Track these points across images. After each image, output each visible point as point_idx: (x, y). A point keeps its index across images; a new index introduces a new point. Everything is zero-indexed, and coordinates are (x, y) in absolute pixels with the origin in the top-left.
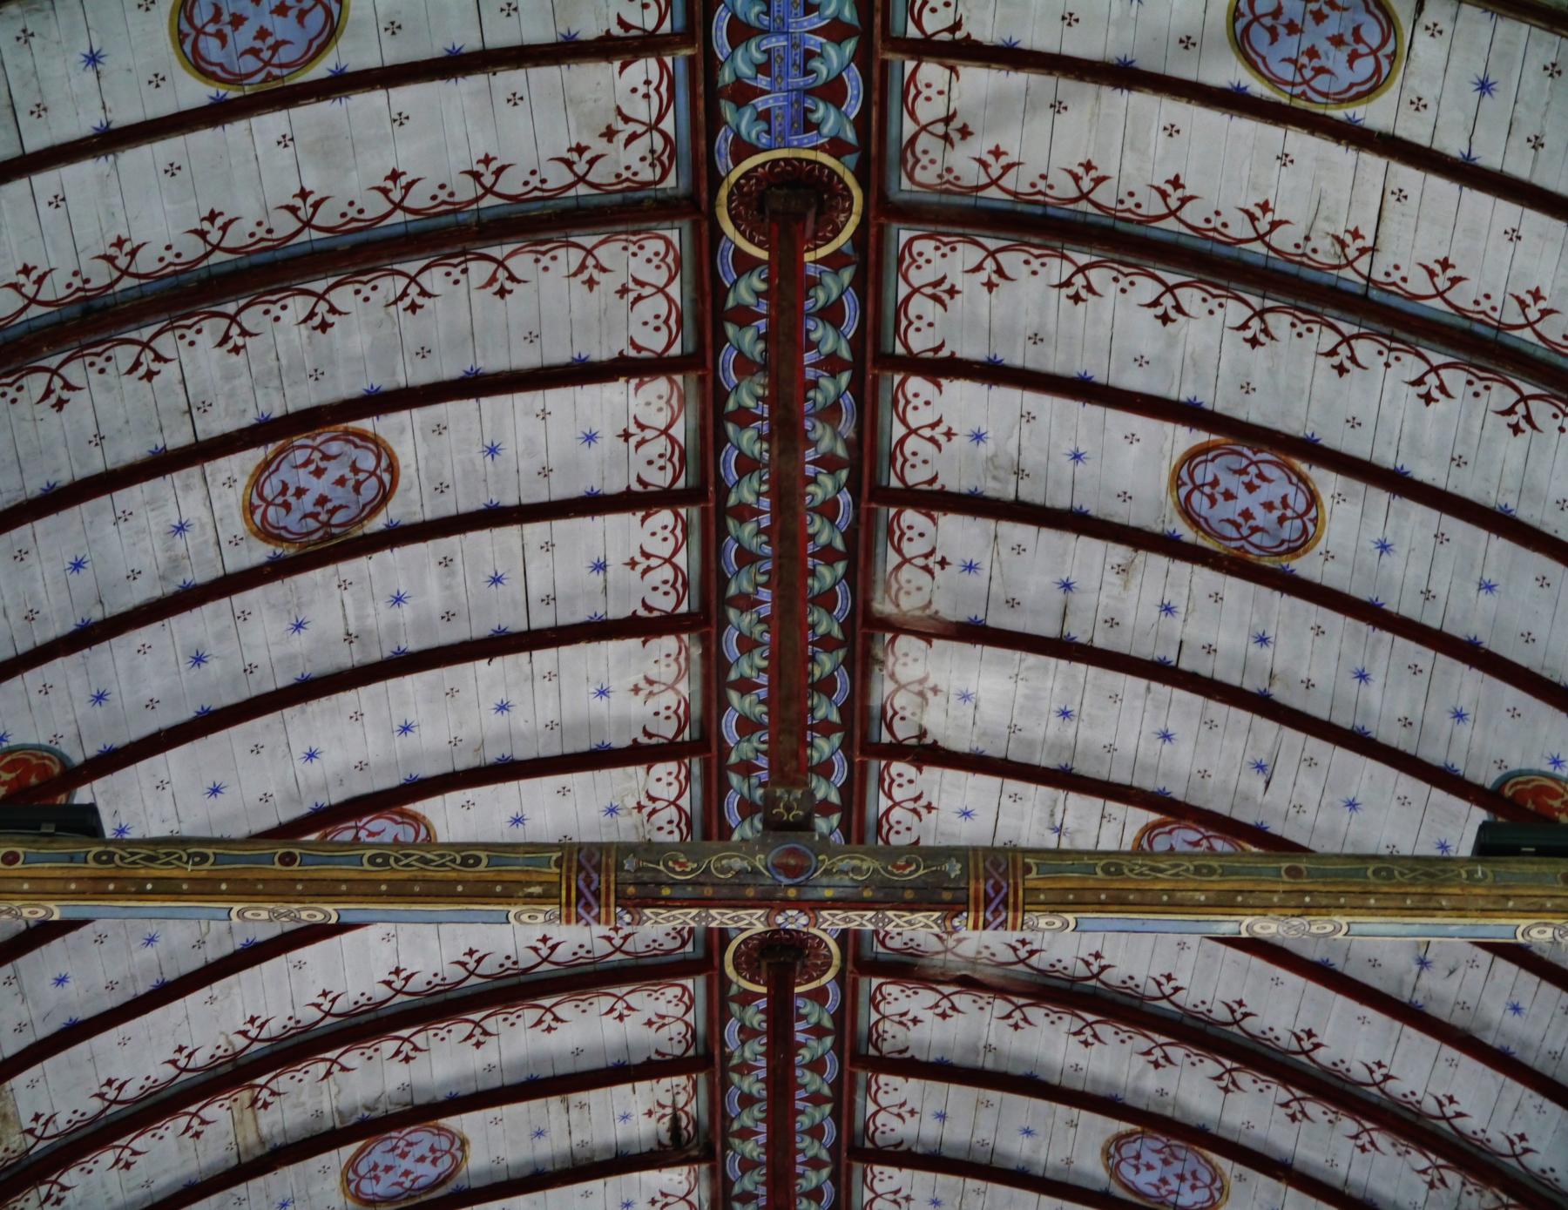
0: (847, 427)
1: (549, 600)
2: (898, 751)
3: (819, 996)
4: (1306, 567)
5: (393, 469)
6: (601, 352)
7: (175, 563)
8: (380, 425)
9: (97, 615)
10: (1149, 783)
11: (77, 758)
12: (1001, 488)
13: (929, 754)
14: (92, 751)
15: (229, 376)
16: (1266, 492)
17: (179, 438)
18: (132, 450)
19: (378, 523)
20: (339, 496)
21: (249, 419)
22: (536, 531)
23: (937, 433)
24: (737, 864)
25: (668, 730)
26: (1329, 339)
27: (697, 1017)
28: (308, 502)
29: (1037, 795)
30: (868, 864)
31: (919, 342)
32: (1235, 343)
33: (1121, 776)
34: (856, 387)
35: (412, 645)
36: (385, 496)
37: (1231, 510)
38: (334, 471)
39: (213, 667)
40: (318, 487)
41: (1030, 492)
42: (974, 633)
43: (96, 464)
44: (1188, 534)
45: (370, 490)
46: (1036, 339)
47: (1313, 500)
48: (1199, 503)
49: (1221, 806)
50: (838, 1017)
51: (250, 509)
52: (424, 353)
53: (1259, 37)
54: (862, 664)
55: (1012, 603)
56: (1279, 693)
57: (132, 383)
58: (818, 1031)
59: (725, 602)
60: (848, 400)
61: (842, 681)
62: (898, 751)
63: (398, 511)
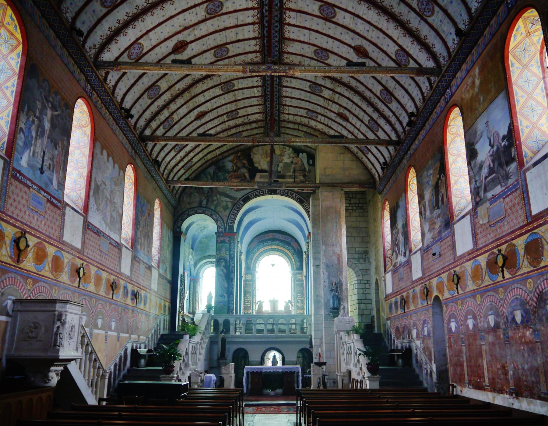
53: (220, 4)
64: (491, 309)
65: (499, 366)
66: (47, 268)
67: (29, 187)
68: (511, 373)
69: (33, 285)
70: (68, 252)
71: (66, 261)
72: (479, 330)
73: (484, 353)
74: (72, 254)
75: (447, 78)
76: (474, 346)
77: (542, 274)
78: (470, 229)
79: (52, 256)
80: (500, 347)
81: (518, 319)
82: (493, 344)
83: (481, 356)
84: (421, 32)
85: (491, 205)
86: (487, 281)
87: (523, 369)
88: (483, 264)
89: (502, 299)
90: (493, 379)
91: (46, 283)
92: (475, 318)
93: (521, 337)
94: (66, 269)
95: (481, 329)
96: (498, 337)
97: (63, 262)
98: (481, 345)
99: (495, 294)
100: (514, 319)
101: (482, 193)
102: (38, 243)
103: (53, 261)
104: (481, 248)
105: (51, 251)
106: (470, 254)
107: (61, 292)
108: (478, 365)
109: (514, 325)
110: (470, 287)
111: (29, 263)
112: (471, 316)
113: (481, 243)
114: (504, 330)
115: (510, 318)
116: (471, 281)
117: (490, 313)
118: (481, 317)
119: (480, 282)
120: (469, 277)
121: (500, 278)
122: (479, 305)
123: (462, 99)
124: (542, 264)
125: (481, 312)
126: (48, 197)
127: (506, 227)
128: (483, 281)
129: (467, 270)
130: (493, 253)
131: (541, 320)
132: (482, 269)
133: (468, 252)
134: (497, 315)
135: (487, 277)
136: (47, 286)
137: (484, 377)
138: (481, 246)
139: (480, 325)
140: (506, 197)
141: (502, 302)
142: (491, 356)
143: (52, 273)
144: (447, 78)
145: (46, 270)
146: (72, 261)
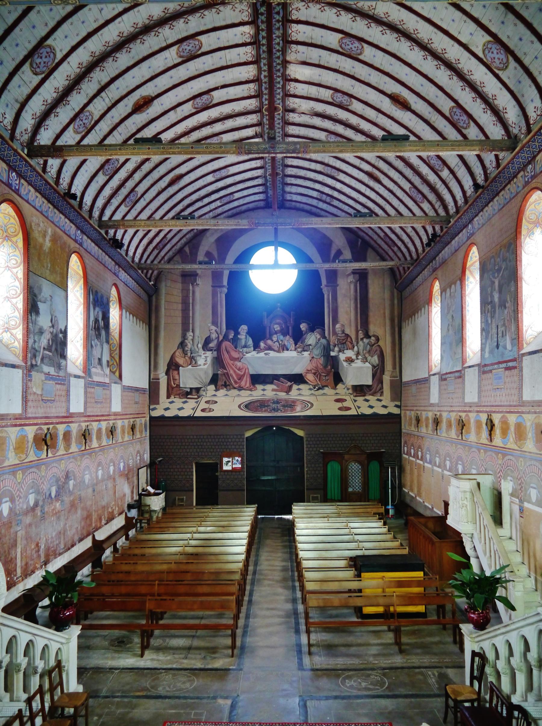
0: (281, 31)
1: (230, 60)
2: (292, 80)
3: (279, 114)
4: (361, 57)
5: (201, 44)
6: (237, 21)
7: (166, 64)
8: (199, 38)
9: (154, 74)
10: (334, 86)
11: (153, 95)
12: (309, 41)
13: (297, 81)
14: (156, 94)
15: (171, 33)
16: (354, 45)
17: (164, 44)
18: (156, 48)
19: (200, 52)
20: (192, 49)
21: (176, 40)
22: (227, 51)
23: (298, 32)
24: (264, 146)
25: (252, 78)
26: (367, 22)
27: (259, 118)
28: (187, 51)
29: (315, 88)
30: (285, 146)
31: (294, 17)
32: (350, 21)
33: (329, 85)
34: (283, 25)
35: (207, 69)
36: (200, 48)
37: (349, 47)
38: (191, 45)
39: (174, 79)
40: (188, 48)
41: (314, 42)
42: (304, 63)
43: (150, 51)
44: (341, 50)
45: (198, 47)
46: (315, 17)
47: (363, 47)
48: (343, 46)
49: (346, 91)
50: (282, 117)
51: (177, 54)
52: (205, 25)
54: (285, 68)
55: (311, 59)
56: (356, 76)
57: (155, 38)
58: (279, 119)
59: (260, 58)
60: (281, 27)
61: (282, 70)
62: (292, 80)
63: (203, 50)
64: (32, 488)
65: (33, 547)
66: (511, 440)
67: (491, 371)
68: (43, 547)
69: (503, 459)
70: (529, 413)
71: (528, 424)
72: (16, 514)
73: (19, 540)
74: (535, 413)
75: (29, 173)
76: (7, 538)
77: (69, 458)
78: (21, 388)
79: (514, 425)
80: (36, 527)
81: (53, 495)
82: (30, 525)
83: (15, 545)
84: (63, 109)
85: (46, 380)
86: (32, 457)
87: (52, 538)
88: (31, 437)
89: (43, 476)
90: (27, 564)
91: (512, 455)
92: (12, 500)
93: (53, 510)
94: (530, 435)
95: (18, 512)
96: (35, 516)
97: (525, 427)
98: (16, 532)
99: (37, 471)
100: (50, 494)
101: (39, 359)
102: (502, 417)
103: (515, 429)
104: (29, 418)
105: (512, 419)
106: (17, 419)
107: (528, 464)
108: (9, 559)
109: (49, 501)
110: (11, 460)
111: (498, 440)
112: (8, 499)
113: (31, 412)
114: (42, 507)
115: (47, 495)
116: (14, 454)
117: (31, 491)
118: (20, 498)
119: (24, 456)
120: (11, 447)
121: (44, 456)
122: (19, 483)
123: (31, 226)
124: (71, 451)
125: (20, 492)
126: (504, 365)
127: (54, 410)
128: (27, 456)
129: (10, 437)
130: (41, 429)
131: (66, 493)
132: (28, 442)
133: (14, 415)
134: (38, 492)
135: (32, 452)
136: (513, 459)
137: (16, 570)
138: (30, 415)
139: (18, 507)
140: (59, 384)
141: (43, 479)
142: (27, 539)
143: (516, 443)
144: (29, 173)
145: (511, 444)
146: (537, 421)
